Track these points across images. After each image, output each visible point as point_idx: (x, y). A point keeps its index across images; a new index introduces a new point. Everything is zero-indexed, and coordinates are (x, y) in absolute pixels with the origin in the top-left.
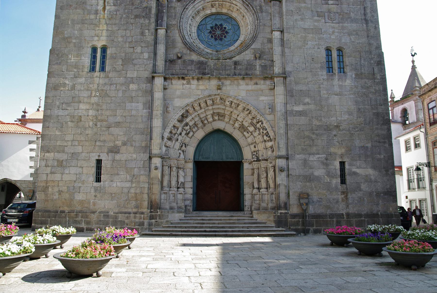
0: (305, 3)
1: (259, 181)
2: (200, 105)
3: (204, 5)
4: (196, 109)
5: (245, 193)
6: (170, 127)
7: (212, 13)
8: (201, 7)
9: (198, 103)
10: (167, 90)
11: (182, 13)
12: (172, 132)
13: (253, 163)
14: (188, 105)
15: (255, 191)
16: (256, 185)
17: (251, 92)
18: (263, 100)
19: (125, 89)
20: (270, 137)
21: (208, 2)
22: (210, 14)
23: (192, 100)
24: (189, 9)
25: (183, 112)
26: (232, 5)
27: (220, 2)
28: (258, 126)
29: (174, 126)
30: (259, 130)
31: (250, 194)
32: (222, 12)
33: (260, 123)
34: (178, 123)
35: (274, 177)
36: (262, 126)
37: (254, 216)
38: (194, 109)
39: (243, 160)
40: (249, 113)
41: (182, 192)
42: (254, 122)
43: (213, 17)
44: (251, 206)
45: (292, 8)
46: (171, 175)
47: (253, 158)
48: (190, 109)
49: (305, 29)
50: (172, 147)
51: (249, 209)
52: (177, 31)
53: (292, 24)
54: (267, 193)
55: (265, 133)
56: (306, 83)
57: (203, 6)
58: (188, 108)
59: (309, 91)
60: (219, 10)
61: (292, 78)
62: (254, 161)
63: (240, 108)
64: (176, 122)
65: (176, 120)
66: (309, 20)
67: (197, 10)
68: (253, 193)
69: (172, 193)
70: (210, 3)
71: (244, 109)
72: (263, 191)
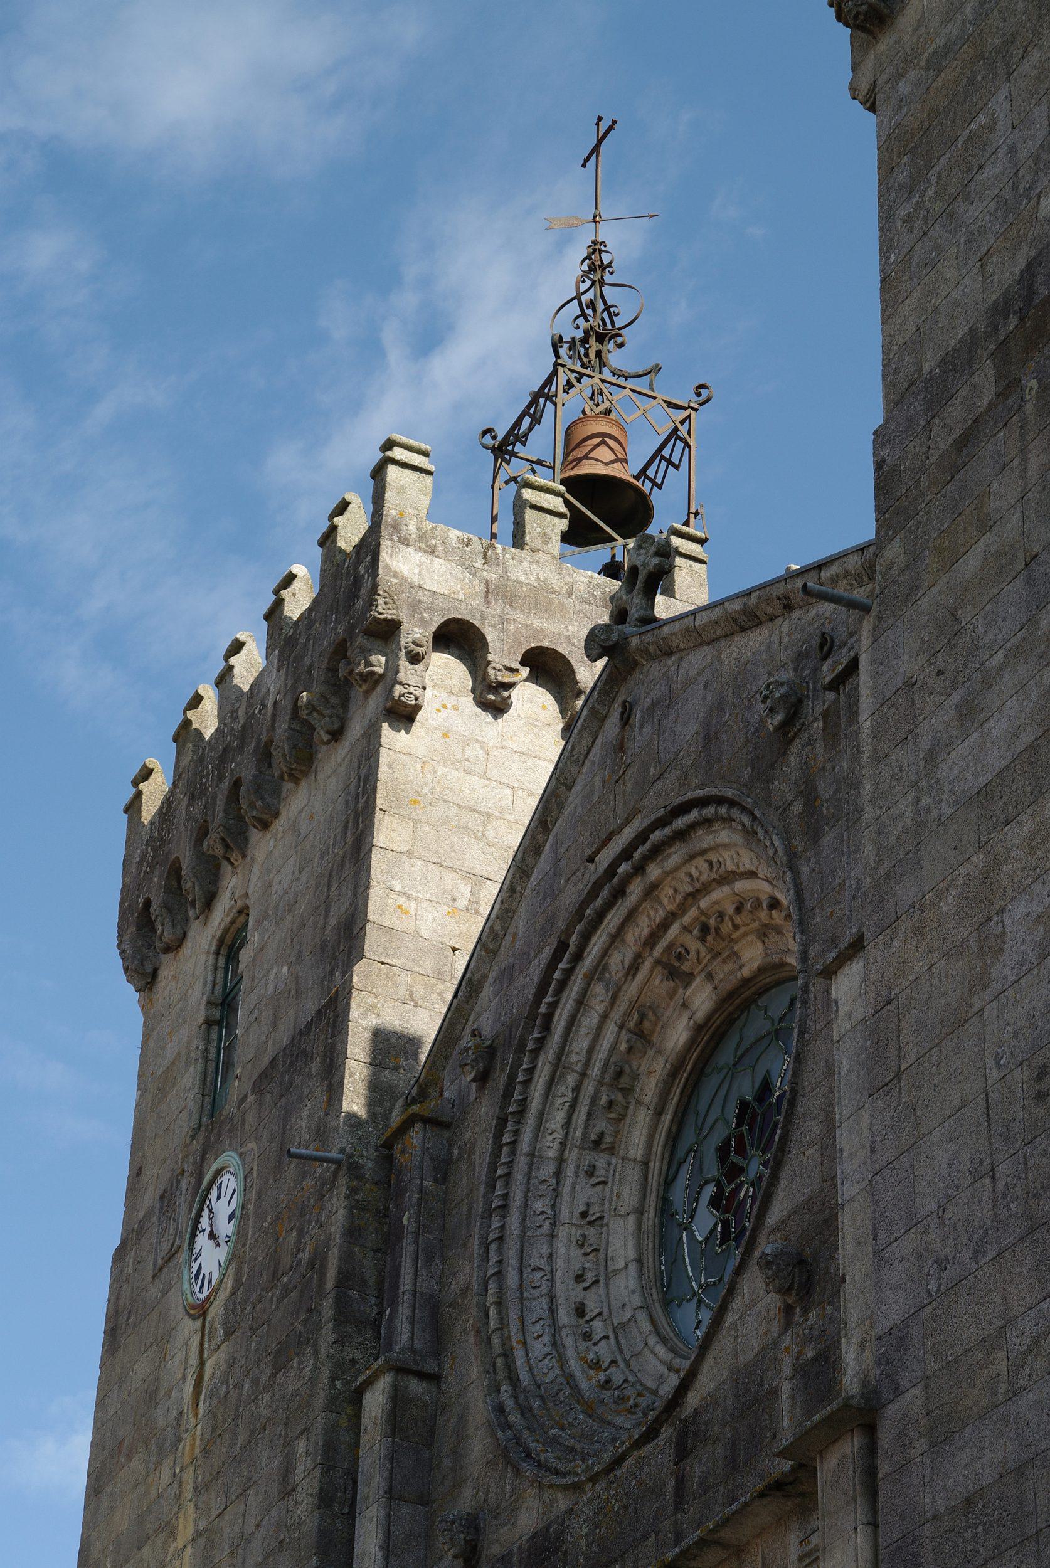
0: (985, 527)
3: (622, 1006)
7: (699, 1029)
8: (610, 1032)
11: (493, 1168)
21: (633, 969)
22: (691, 1044)
24: (534, 1105)
26: (741, 886)
27: (687, 919)
32: (746, 982)
43: (726, 1056)
45: (908, 665)
49: (985, 793)
52: (471, 1338)
53: (909, 816)
56: (1003, 1387)
57: (616, 1015)
59: (1019, 1471)
60: (727, 974)
61: (913, 1396)
66: (1007, 675)
67: (595, 1071)
70: (647, 965)
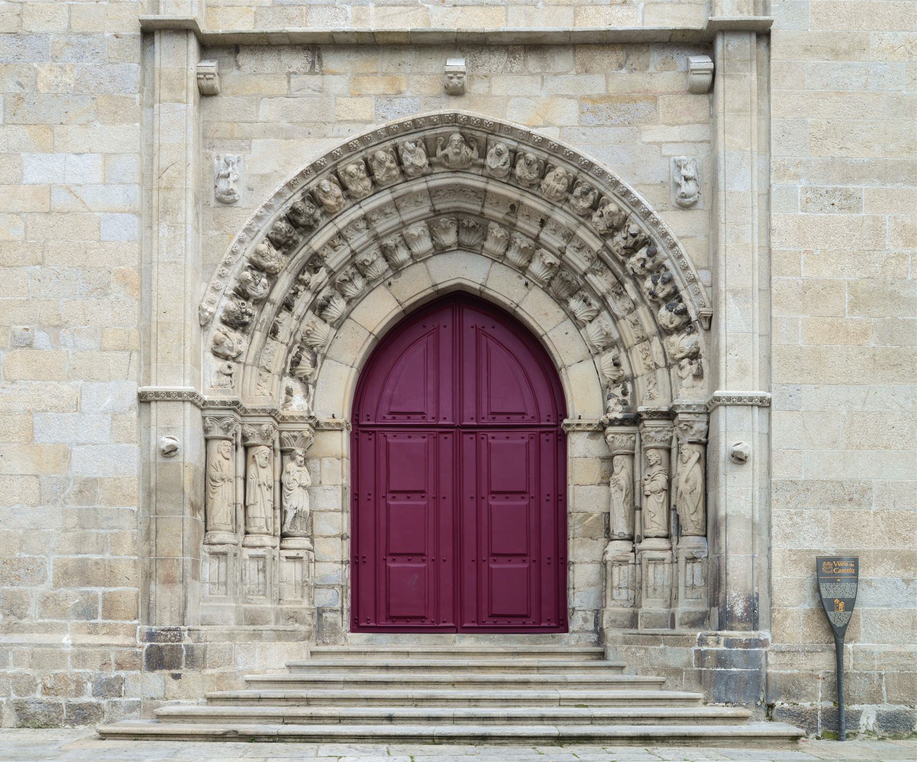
1: (635, 508)
2: (370, 172)
4: (352, 188)
5: (571, 558)
6: (236, 268)
9: (358, 157)
10: (215, 99)
12: (244, 291)
13: (610, 429)
14: (315, 168)
15: (618, 549)
16: (620, 526)
17: (603, 106)
18: (659, 144)
19: (18, 89)
20: (684, 312)
23: (334, 144)
25: (290, 204)
28: (633, 262)
29: (255, 266)
30: (636, 278)
31: (593, 562)
33: (643, 253)
34: (274, 252)
35: (699, 488)
36: (648, 266)
37: (611, 654)
38: (344, 188)
39: (566, 421)
40: (594, 207)
41: (302, 554)
42: (614, 249)
44: (598, 614)
46: (249, 480)
47: (607, 411)
48: (326, 185)
50: (250, 361)
51: (590, 626)
54: (667, 555)
55: (661, 295)
58: (315, 182)
62: (612, 422)
63: (554, 182)
64: (264, 247)
65: (261, 236)
68: (608, 557)
69: (252, 557)
71: (570, 189)
72: (653, 546)
